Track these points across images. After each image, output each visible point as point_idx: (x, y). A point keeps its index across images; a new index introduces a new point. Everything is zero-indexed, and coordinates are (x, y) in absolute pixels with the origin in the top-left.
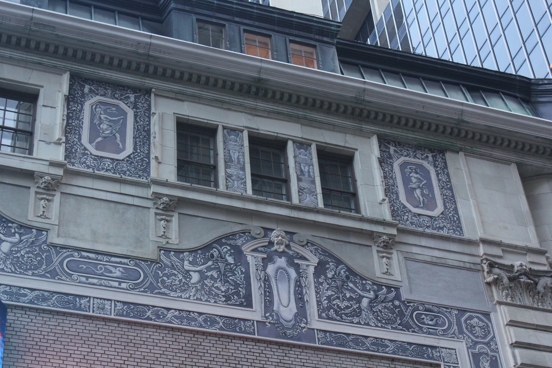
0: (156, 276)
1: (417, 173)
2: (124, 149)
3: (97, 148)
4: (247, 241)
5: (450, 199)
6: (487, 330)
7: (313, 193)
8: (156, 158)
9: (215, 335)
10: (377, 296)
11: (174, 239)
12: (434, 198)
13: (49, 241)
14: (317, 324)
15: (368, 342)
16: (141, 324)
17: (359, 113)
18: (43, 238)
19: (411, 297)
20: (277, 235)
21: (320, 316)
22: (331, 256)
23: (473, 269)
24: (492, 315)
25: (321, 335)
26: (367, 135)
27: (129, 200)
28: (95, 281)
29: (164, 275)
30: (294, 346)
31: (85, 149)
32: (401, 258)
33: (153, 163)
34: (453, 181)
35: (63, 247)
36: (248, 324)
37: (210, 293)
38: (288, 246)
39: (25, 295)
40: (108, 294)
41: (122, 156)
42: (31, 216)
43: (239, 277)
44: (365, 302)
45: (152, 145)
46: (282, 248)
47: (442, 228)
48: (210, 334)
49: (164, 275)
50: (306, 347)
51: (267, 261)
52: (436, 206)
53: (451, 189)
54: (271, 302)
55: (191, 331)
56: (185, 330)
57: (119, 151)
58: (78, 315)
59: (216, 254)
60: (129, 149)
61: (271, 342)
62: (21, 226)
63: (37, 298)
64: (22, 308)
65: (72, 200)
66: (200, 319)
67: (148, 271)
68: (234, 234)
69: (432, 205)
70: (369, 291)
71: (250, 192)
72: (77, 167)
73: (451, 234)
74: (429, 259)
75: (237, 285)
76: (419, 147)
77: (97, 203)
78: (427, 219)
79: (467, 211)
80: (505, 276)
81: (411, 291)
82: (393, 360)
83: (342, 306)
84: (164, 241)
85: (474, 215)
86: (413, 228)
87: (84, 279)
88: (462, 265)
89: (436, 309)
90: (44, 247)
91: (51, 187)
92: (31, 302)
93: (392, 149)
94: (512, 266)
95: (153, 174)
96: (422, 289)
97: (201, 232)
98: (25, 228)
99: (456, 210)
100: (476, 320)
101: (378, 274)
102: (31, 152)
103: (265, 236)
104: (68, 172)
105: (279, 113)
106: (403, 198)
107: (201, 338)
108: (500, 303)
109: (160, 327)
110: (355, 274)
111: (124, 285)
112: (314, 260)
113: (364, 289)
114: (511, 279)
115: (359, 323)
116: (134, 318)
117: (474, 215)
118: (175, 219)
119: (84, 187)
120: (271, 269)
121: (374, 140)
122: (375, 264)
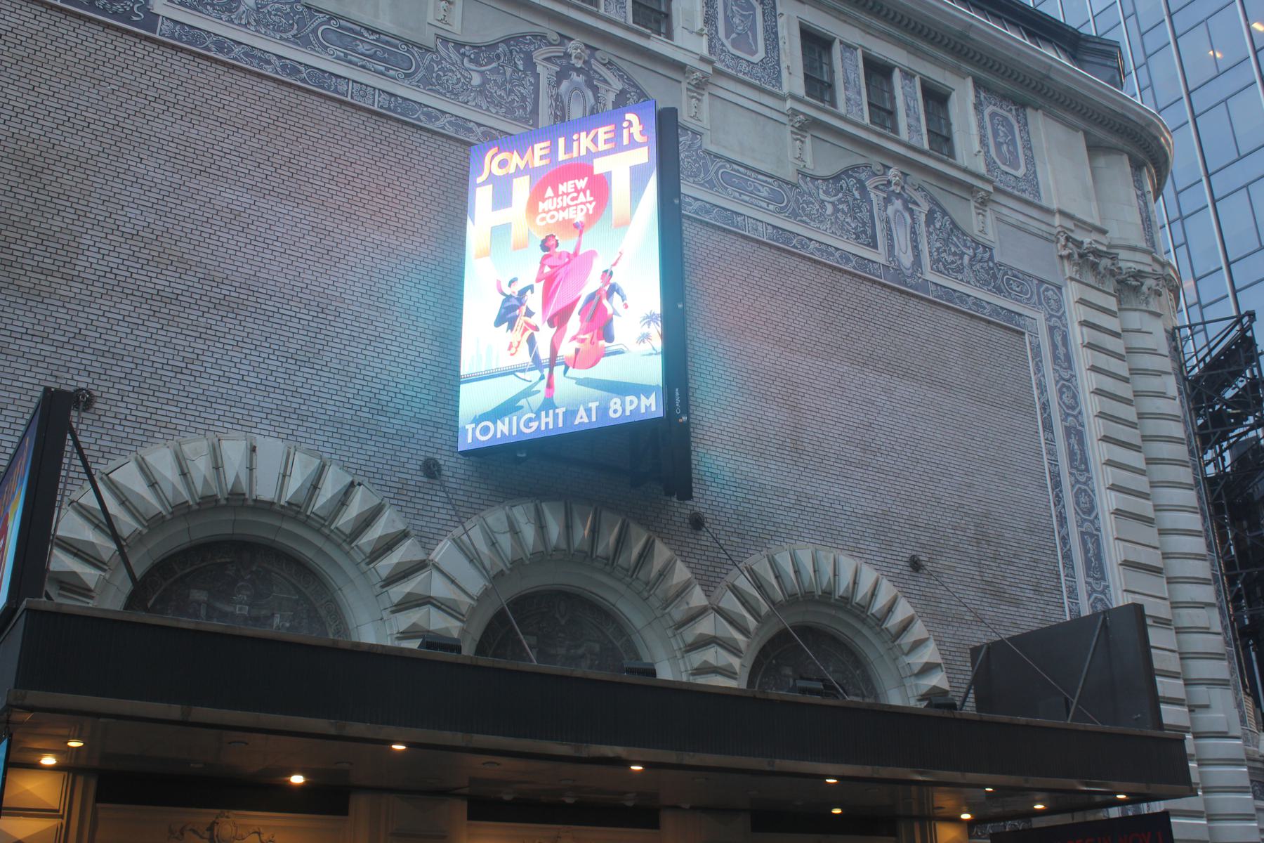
0: (797, 201)
3: (735, 44)
4: (870, 177)
5: (1030, 161)
6: (1059, 303)
7: (918, 131)
9: (849, 273)
12: (1017, 157)
13: (704, 147)
14: (930, 276)
15: (970, 300)
17: (960, 49)
20: (893, 173)
22: (938, 205)
23: (1051, 239)
24: (1063, 290)
26: (962, 75)
28: (747, 198)
31: (723, 45)
33: (784, 73)
34: (1033, 140)
35: (717, 156)
36: (876, 266)
38: (903, 188)
40: (761, 216)
43: (865, 215)
44: (966, 259)
47: (1024, 191)
53: (1030, 149)
54: (893, 246)
55: (830, 266)
56: (825, 265)
57: (754, 53)
58: (736, 234)
59: (844, 186)
60: (761, 54)
66: (837, 254)
69: (1017, 167)
71: (867, 120)
73: (1030, 198)
75: (864, 224)
76: (1005, 97)
79: (1046, 176)
80: (1076, 251)
82: (989, 322)
84: (802, 164)
85: (1051, 183)
86: (1002, 186)
93: (982, 95)
94: (1082, 243)
96: (1014, 253)
99: (1035, 172)
101: (976, 232)
102: (669, 35)
105: (890, 35)
108: (1072, 279)
109: (804, 257)
111: (771, 207)
112: (925, 207)
113: (965, 246)
114: (1081, 256)
116: (782, 246)
117: (1051, 183)
118: (808, 141)
121: (969, 82)
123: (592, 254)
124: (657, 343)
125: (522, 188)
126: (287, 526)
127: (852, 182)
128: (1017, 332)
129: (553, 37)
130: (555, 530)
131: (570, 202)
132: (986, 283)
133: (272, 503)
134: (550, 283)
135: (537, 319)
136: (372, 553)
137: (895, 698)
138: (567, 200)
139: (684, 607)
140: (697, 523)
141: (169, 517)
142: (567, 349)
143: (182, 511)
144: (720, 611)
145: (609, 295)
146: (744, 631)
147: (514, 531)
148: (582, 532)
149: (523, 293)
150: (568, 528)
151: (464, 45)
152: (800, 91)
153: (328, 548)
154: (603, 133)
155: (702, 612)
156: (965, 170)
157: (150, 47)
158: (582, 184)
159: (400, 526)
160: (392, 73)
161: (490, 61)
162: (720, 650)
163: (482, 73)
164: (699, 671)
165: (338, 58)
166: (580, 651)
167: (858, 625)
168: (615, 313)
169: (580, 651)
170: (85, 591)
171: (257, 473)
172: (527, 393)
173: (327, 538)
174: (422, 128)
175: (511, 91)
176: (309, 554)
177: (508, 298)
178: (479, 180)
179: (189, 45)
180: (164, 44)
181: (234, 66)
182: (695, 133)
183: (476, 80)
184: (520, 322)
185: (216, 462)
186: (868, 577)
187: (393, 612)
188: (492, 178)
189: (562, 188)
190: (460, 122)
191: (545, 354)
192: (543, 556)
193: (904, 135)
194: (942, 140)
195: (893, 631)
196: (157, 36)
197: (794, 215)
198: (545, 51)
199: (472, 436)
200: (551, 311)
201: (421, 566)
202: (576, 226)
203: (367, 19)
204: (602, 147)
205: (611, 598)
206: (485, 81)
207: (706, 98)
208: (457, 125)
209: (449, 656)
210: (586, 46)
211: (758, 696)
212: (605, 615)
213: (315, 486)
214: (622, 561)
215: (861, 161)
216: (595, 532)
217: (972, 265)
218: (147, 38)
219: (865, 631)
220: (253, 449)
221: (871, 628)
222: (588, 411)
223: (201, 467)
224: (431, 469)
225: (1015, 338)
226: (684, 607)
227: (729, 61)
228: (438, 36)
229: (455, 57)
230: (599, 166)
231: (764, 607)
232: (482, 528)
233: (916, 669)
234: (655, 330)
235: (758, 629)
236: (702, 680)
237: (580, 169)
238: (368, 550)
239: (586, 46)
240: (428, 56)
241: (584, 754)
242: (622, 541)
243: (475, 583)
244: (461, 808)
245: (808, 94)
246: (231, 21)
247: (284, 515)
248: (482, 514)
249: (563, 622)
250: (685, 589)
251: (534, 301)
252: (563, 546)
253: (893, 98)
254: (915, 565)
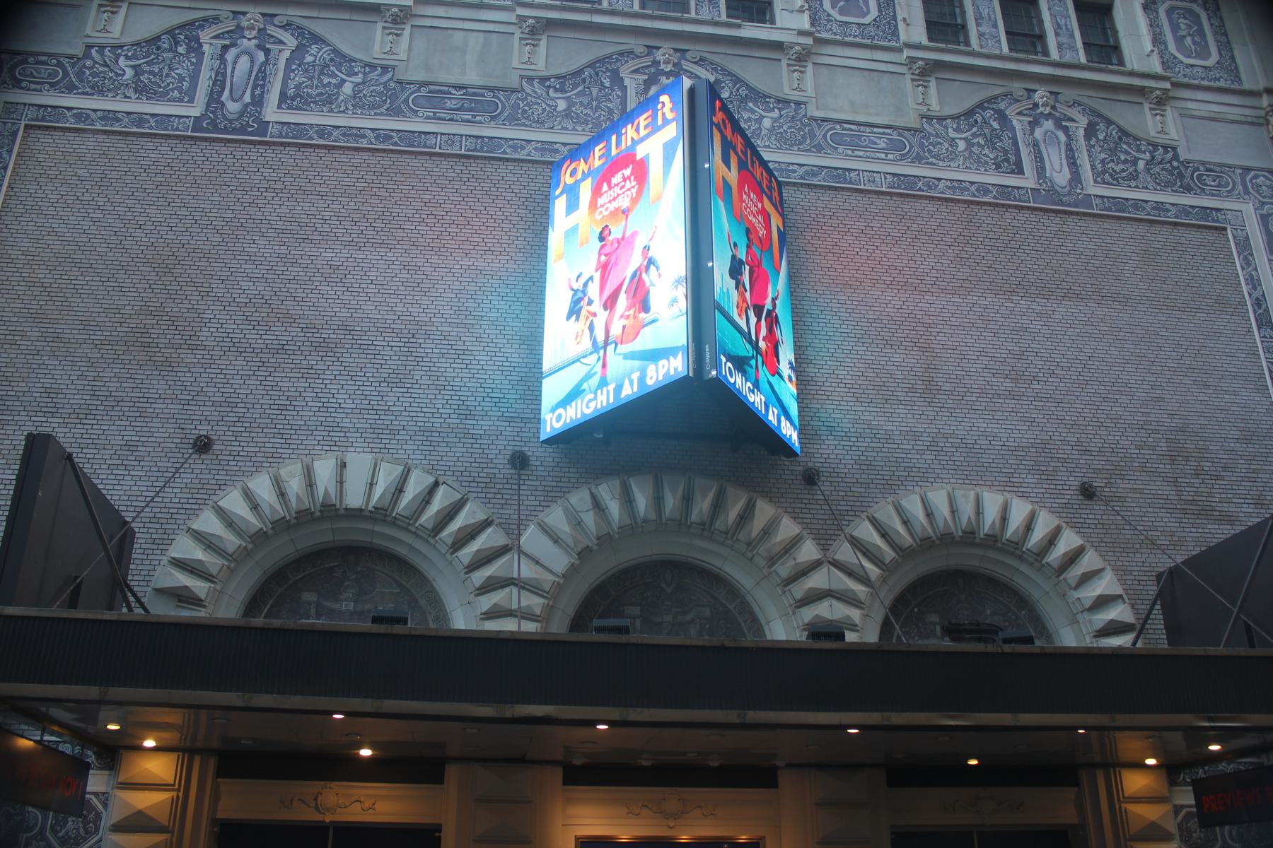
0: (922, 145)
1: (1185, 18)
2: (868, 12)
3: (841, 14)
4: (1010, 104)
7: (1073, 48)
8: (904, 19)
9: (990, 204)
10: (1153, 158)
11: (935, 106)
12: (1207, 45)
13: (809, 114)
14: (1093, 189)
15: (1148, 207)
16: (914, 196)
18: (802, 112)
19: (1190, 157)
20: (1040, 95)
21: (1095, 181)
22: (1100, 116)
25: (1098, 201)
27: (883, 67)
29: (930, 144)
30: (1072, 213)
31: (829, 15)
32: (1176, 115)
33: (901, 25)
36: (1022, 192)
37: (979, 162)
38: (1053, 108)
39: (795, 171)
40: (876, 167)
41: (867, 20)
42: (787, 90)
43: (1007, 143)
44: (1141, 164)
45: (897, 7)
46: (1048, 110)
47: (1218, 80)
48: (985, 204)
49: (930, 144)
50: (1085, 214)
51: (1034, 124)
52: (1210, 55)
54: (1043, 168)
55: (965, 202)
56: (959, 201)
57: (864, 15)
58: (849, 189)
59: (980, 119)
60: (874, 13)
61: (1047, 210)
62: (779, 101)
63: (807, 173)
64: (794, 184)
65: (825, 70)
67: (913, 141)
68: (995, 97)
69: (1204, 54)
70: (1144, 152)
71: (1006, 50)
72: (824, 35)
74: (1206, 115)
75: (1005, 152)
77: (851, 71)
78: (1200, 70)
81: (1189, 150)
82: (1176, 224)
83: (1119, 168)
86: (1186, 80)
87: (850, 152)
88: (1243, 119)
89: (1217, 169)
90: (805, 121)
91: (802, 58)
92: (801, 178)
95: (903, 37)
96: (1203, 146)
97: (963, 96)
98: (783, 102)
100: (1262, 178)
101: (1153, 133)
102: (772, 21)
103: (1029, 98)
104: (819, 42)
106: (1172, 47)
107: (976, 208)
109: (933, 198)
110: (1127, 134)
111: (890, 157)
112: (1083, 121)
113: (1139, 151)
115: (1137, 187)
116: (905, 191)
118: (933, 84)
119: (834, 56)
120: (1038, 133)
122: (1146, 123)
123: (634, 234)
124: (682, 304)
125: (586, 189)
126: (378, 528)
127: (989, 113)
128: (1216, 228)
129: (640, 50)
130: (642, 502)
132: (1169, 184)
133: (361, 510)
135: (597, 307)
136: (454, 544)
137: (1068, 638)
138: (617, 190)
139: (791, 563)
140: (811, 478)
141: (270, 532)
142: (616, 331)
143: (281, 526)
144: (836, 564)
145: (647, 268)
146: (864, 580)
147: (598, 506)
148: (671, 502)
149: (585, 285)
150: (658, 501)
151: (548, 79)
152: (924, 40)
153: (418, 544)
155: (815, 566)
156: (1132, 74)
157: (262, 148)
158: (627, 172)
159: (481, 516)
160: (478, 118)
161: (575, 86)
162: (834, 602)
163: (567, 99)
164: (491, 615)
165: (428, 118)
166: (689, 617)
167: (1015, 563)
168: (652, 284)
169: (689, 617)
170: (195, 601)
171: (347, 485)
172: (588, 376)
173: (415, 533)
174: (508, 160)
175: (598, 108)
176: (403, 551)
177: (576, 291)
178: (557, 192)
179: (296, 140)
180: (274, 144)
181: (334, 147)
182: (798, 104)
183: (562, 105)
184: (584, 313)
185: (310, 480)
186: (1019, 512)
187: (477, 595)
189: (614, 181)
190: (548, 147)
191: (600, 338)
192: (634, 528)
193: (1054, 55)
194: (1104, 47)
195: (1055, 565)
196: (268, 139)
197: (919, 159)
198: (632, 64)
200: (605, 296)
201: (504, 550)
202: (623, 212)
203: (452, 79)
205: (718, 563)
206: (571, 104)
207: (810, 66)
208: (544, 150)
209: (397, 629)
210: (676, 50)
211: (727, 644)
212: (717, 580)
213: (400, 490)
214: (719, 524)
215: (998, 91)
216: (688, 500)
217: (1148, 170)
218: (260, 143)
219: (1023, 568)
220: (344, 465)
221: (1031, 564)
222: (631, 382)
223: (295, 486)
224: (520, 461)
225: (1212, 236)
226: (791, 563)
227: (835, 28)
228: (522, 77)
229: (539, 90)
230: (640, 153)
231: (889, 554)
232: (566, 510)
233: (1088, 604)
235: (884, 580)
236: (492, 626)
237: (627, 159)
238: (450, 541)
239: (676, 50)
240: (514, 96)
241: (508, 715)
242: (718, 506)
243: (559, 561)
244: (559, 773)
245: (930, 39)
246: (332, 111)
247: (376, 520)
248: (567, 496)
249: (669, 590)
250: (795, 542)
251: (593, 290)
252: (652, 516)
253: (1041, 21)
254: (1087, 492)
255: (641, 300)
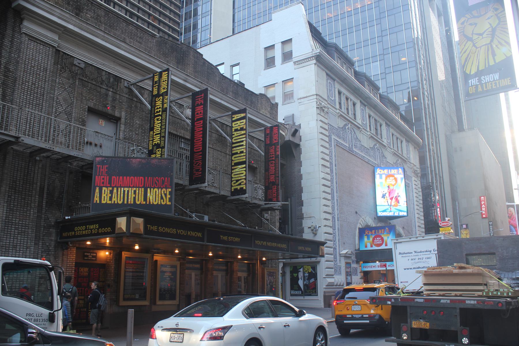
125: (384, 176)
131: (391, 181)
134: (390, 193)
135: (388, 198)
154: (396, 170)
172: (387, 209)
188: (379, 174)
191: (390, 204)
199: (380, 214)
200: (391, 196)
204: (396, 173)
230: (396, 176)
234: (406, 203)
251: (387, 195)
254: (403, 228)
255: (397, 201)
